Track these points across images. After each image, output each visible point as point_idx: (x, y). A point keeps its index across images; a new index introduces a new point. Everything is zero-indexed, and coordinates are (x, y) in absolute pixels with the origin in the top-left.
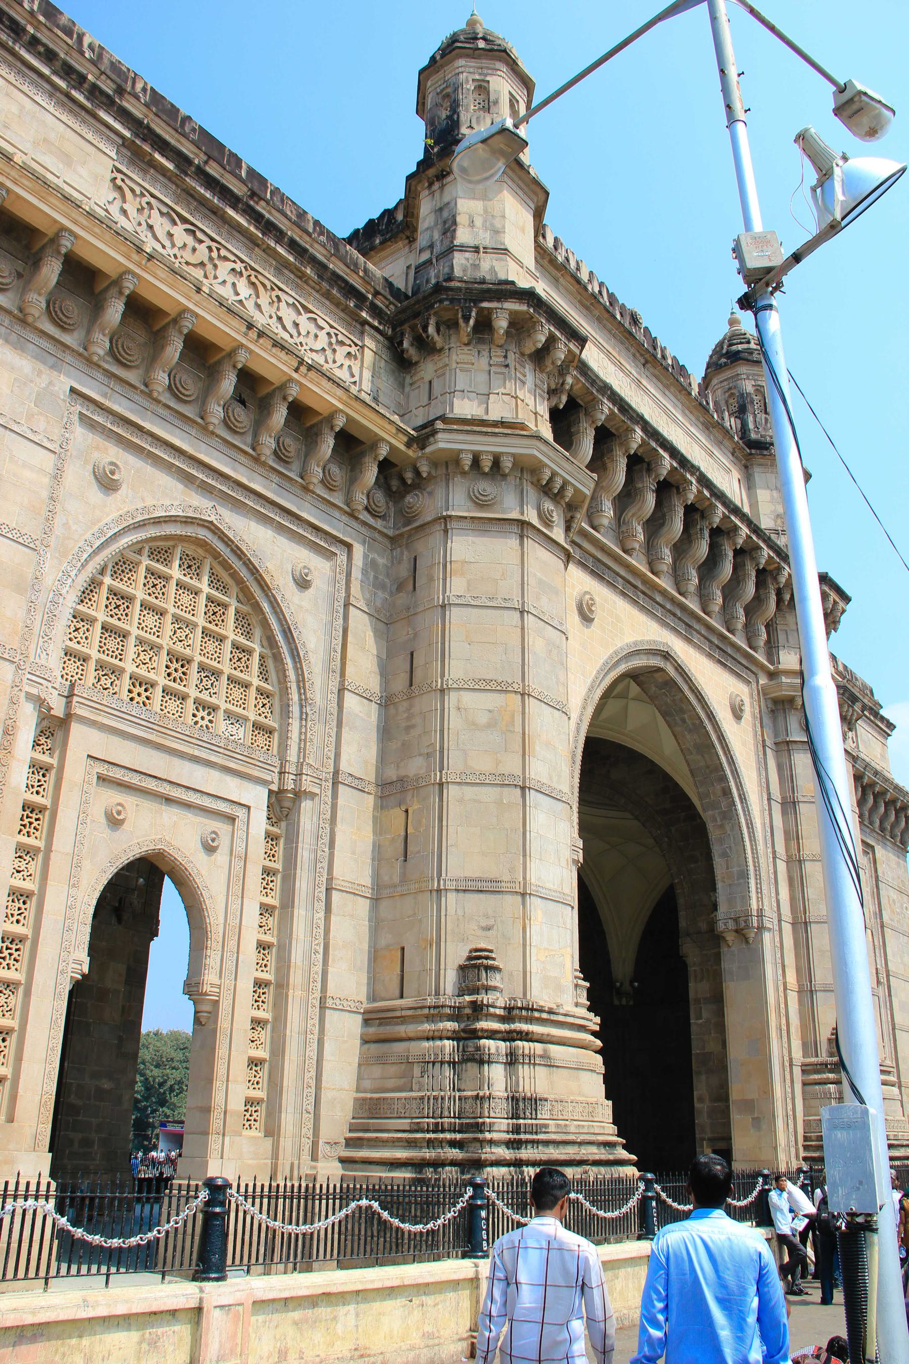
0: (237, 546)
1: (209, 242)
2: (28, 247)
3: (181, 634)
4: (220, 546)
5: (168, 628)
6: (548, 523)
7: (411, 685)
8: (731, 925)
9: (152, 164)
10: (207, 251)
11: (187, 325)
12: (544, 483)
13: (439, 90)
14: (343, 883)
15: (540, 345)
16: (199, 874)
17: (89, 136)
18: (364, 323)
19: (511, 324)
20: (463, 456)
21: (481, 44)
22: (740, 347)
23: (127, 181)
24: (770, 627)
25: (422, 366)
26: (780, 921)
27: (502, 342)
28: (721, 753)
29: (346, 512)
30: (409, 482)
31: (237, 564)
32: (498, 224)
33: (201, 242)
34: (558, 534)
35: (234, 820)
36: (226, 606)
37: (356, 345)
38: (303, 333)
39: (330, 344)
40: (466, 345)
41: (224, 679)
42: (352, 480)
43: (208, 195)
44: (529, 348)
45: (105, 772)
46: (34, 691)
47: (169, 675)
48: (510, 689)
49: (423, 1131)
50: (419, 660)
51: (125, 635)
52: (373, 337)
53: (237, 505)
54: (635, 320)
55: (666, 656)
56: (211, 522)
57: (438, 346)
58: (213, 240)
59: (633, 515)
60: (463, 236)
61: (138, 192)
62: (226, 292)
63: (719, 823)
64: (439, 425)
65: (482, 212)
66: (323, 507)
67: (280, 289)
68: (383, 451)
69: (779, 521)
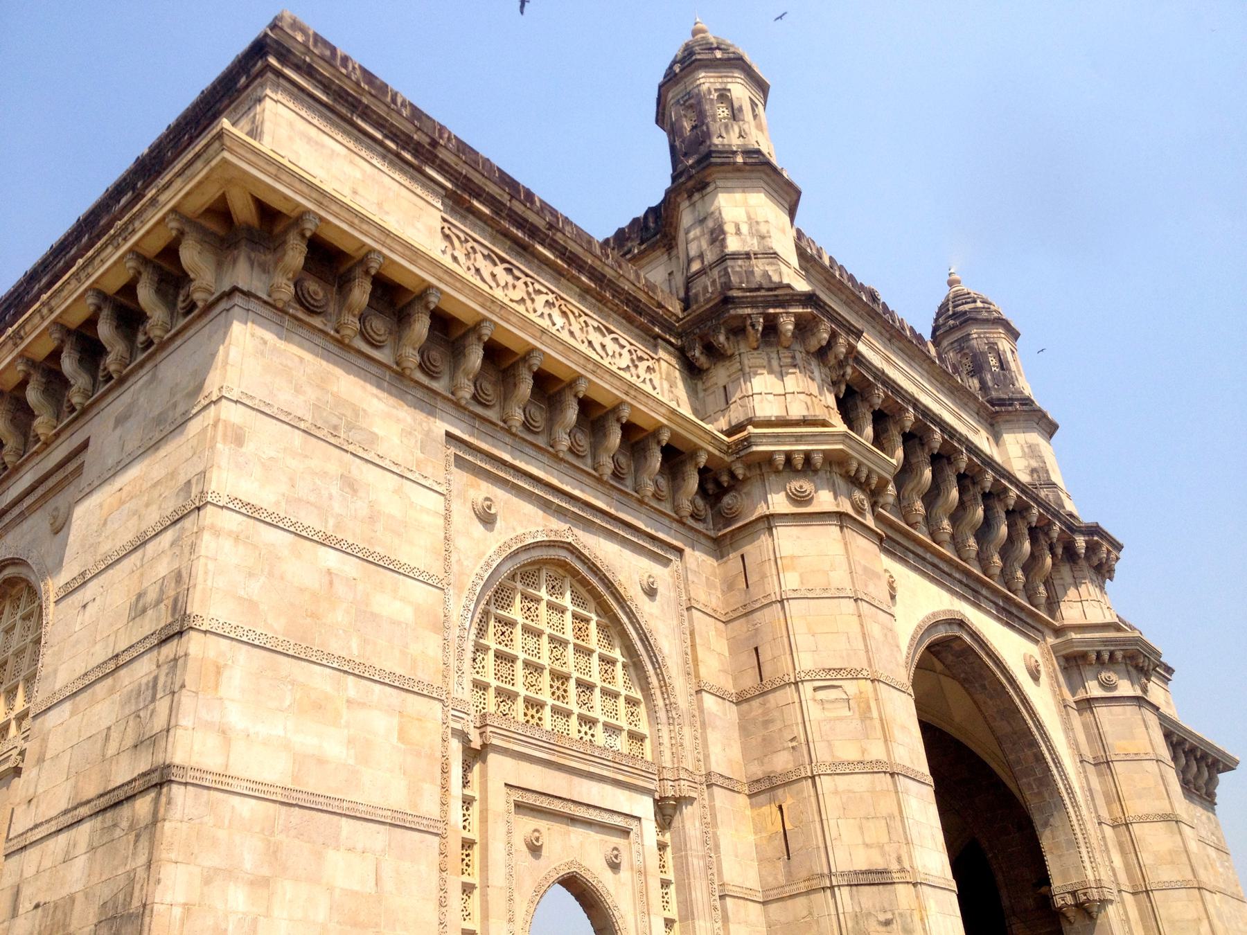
0: (593, 563)
1: (524, 279)
2: (392, 304)
3: (557, 653)
7: (761, 680)
8: (1070, 900)
10: (524, 286)
11: (536, 363)
12: (853, 474)
14: (734, 888)
15: (824, 343)
19: (797, 325)
21: (719, 54)
22: (967, 307)
24: (1048, 583)
25: (713, 372)
26: (1120, 891)
27: (786, 344)
28: (1027, 717)
30: (726, 485)
31: (594, 581)
32: (763, 229)
33: (518, 279)
34: (870, 521)
37: (653, 358)
39: (632, 360)
40: (755, 349)
42: (675, 489)
43: (520, 234)
44: (814, 344)
45: (520, 799)
46: (458, 726)
47: (553, 693)
48: (860, 676)
52: (665, 349)
53: (588, 525)
54: (873, 297)
55: (961, 624)
56: (570, 544)
57: (729, 352)
58: (527, 275)
60: (733, 245)
61: (463, 239)
62: (545, 323)
63: (1036, 791)
64: (751, 429)
65: (746, 220)
66: (655, 516)
67: (586, 315)
68: (703, 460)
69: (1035, 476)
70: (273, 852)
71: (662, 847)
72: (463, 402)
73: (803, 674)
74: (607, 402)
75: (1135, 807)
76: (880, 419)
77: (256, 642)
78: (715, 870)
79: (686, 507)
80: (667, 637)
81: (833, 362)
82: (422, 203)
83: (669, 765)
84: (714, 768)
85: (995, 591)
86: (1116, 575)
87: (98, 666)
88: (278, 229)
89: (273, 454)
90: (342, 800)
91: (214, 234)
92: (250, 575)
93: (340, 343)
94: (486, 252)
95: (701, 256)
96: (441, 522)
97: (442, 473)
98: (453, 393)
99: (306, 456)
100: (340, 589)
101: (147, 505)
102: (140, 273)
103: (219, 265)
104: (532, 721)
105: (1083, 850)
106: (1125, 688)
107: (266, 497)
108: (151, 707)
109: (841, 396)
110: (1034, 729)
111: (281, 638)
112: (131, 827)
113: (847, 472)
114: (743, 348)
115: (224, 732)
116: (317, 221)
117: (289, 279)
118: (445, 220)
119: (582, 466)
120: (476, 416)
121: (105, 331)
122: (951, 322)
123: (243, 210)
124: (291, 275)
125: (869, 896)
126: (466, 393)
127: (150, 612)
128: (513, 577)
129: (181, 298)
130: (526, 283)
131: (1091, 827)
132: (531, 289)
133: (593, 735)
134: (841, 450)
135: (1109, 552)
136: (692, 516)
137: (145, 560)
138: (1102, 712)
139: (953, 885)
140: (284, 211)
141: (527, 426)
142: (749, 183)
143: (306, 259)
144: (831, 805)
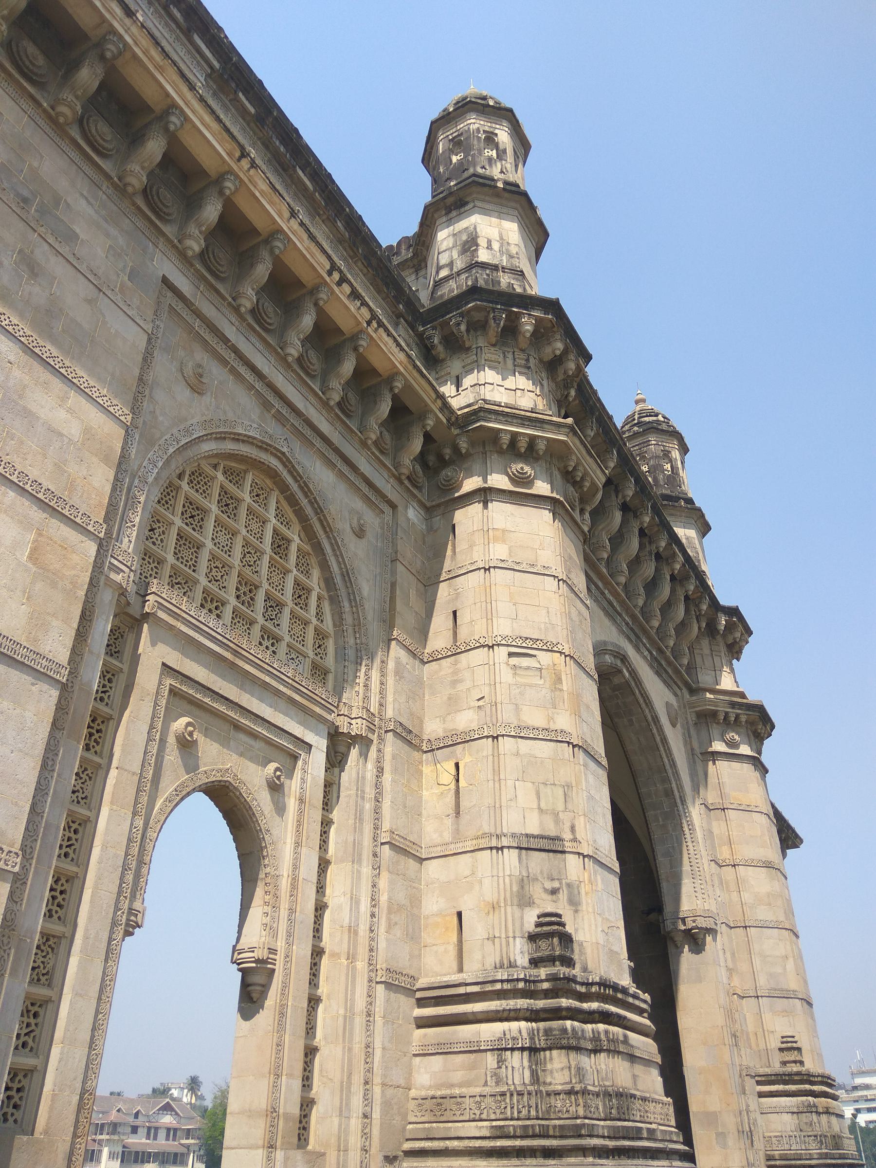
0: (304, 482)
4: (290, 480)
13: (450, 137)
15: (558, 353)
16: (263, 814)
24: (691, 649)
25: (449, 363)
29: (394, 475)
31: (304, 502)
36: (289, 541)
42: (398, 448)
48: (555, 649)
55: (624, 659)
56: (283, 454)
57: (467, 345)
63: (661, 823)
65: (498, 239)
74: (346, 325)
80: (368, 581)
81: (561, 377)
86: (743, 656)
110: (668, 767)
113: (566, 467)
114: (481, 342)
122: (636, 428)
125: (538, 861)
136: (408, 478)
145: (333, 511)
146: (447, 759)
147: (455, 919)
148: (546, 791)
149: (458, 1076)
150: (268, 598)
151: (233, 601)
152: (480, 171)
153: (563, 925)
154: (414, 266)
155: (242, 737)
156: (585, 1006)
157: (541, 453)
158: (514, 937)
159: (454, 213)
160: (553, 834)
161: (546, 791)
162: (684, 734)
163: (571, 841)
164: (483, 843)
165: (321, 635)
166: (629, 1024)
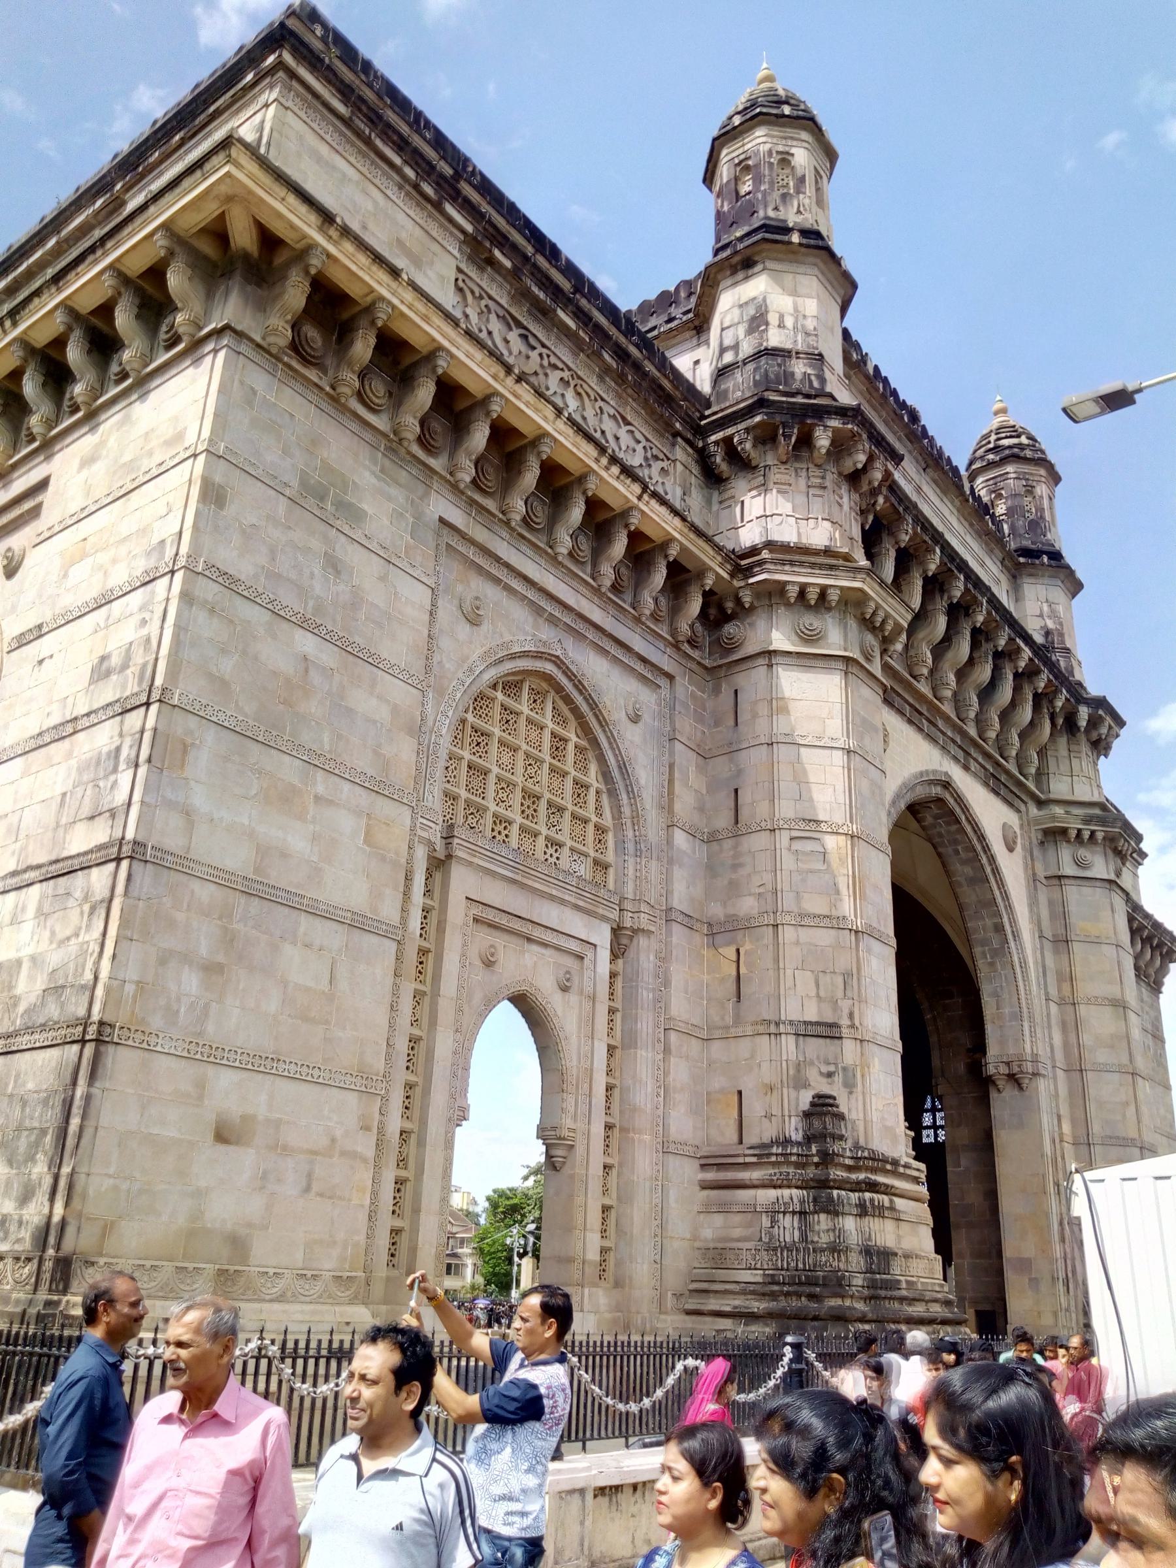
1: (540, 349)
2: (396, 363)
4: (564, 681)
5: (520, 763)
6: (868, 659)
7: (737, 822)
9: (491, 262)
11: (546, 450)
12: (868, 617)
13: (737, 161)
15: (860, 466)
17: (434, 234)
18: (676, 434)
19: (834, 442)
20: (789, 587)
21: (787, 110)
23: (467, 281)
24: (1042, 753)
26: (1054, 1067)
27: (819, 462)
29: (670, 643)
31: (579, 700)
35: (582, 958)
36: (565, 740)
37: (668, 459)
38: (624, 448)
39: (646, 459)
40: (783, 463)
41: (567, 815)
42: (675, 610)
43: (542, 295)
44: (848, 466)
46: (425, 834)
47: (523, 812)
48: (841, 831)
49: (778, 1283)
50: (745, 797)
51: (486, 773)
53: (579, 636)
55: (947, 785)
56: (557, 657)
57: (754, 463)
58: (544, 346)
59: (923, 639)
61: (477, 294)
65: (792, 311)
66: (649, 638)
67: (603, 399)
68: (709, 582)
70: (229, 939)
71: (613, 975)
72: (462, 486)
73: (781, 822)
74: (615, 503)
75: (1086, 989)
76: (905, 560)
77: (226, 724)
78: (662, 1005)
79: (684, 627)
80: (645, 767)
81: (865, 488)
82: (435, 247)
83: (630, 896)
84: (676, 903)
85: (987, 756)
86: (1112, 753)
87: (55, 727)
88: (280, 259)
89: (254, 521)
90: (303, 897)
91: (206, 258)
92: (224, 651)
93: (335, 400)
94: (501, 313)
95: (736, 347)
96: (426, 617)
97: (431, 564)
98: (451, 474)
99: (290, 528)
100: (315, 678)
101: (114, 561)
102: (120, 294)
103: (210, 295)
104: (499, 837)
105: (1026, 1025)
106: (1101, 867)
107: (244, 568)
108: (112, 778)
109: (867, 527)
110: (999, 900)
111: (251, 723)
112: (86, 898)
113: (863, 614)
114: (770, 460)
115: (187, 814)
116: (324, 257)
117: (287, 322)
118: (459, 270)
119: (581, 574)
120: (472, 502)
121: (74, 354)
122: (991, 457)
123: (243, 237)
124: (289, 317)
125: (814, 1047)
126: (466, 475)
127: (114, 677)
128: (494, 687)
129: (164, 328)
130: (541, 355)
131: (1038, 1003)
132: (545, 363)
133: (558, 858)
134: (860, 590)
135: (1110, 727)
136: (689, 642)
137: (111, 621)
138: (1072, 892)
139: (899, 1046)
140: (289, 241)
141: (526, 521)
142: (802, 269)
143: (309, 298)
144: (791, 956)
145: (608, 703)
146: (728, 944)
147: (736, 1098)
148: (825, 980)
149: (737, 1232)
150: (550, 804)
151: (519, 819)
152: (771, 214)
153: (837, 1107)
154: (695, 328)
155: (535, 948)
156: (854, 1176)
157: (834, 604)
158: (790, 1116)
159: (741, 275)
160: (830, 1021)
161: (825, 980)
162: (1025, 858)
163: (849, 1027)
164: (761, 1029)
165: (600, 829)
166: (897, 1192)
